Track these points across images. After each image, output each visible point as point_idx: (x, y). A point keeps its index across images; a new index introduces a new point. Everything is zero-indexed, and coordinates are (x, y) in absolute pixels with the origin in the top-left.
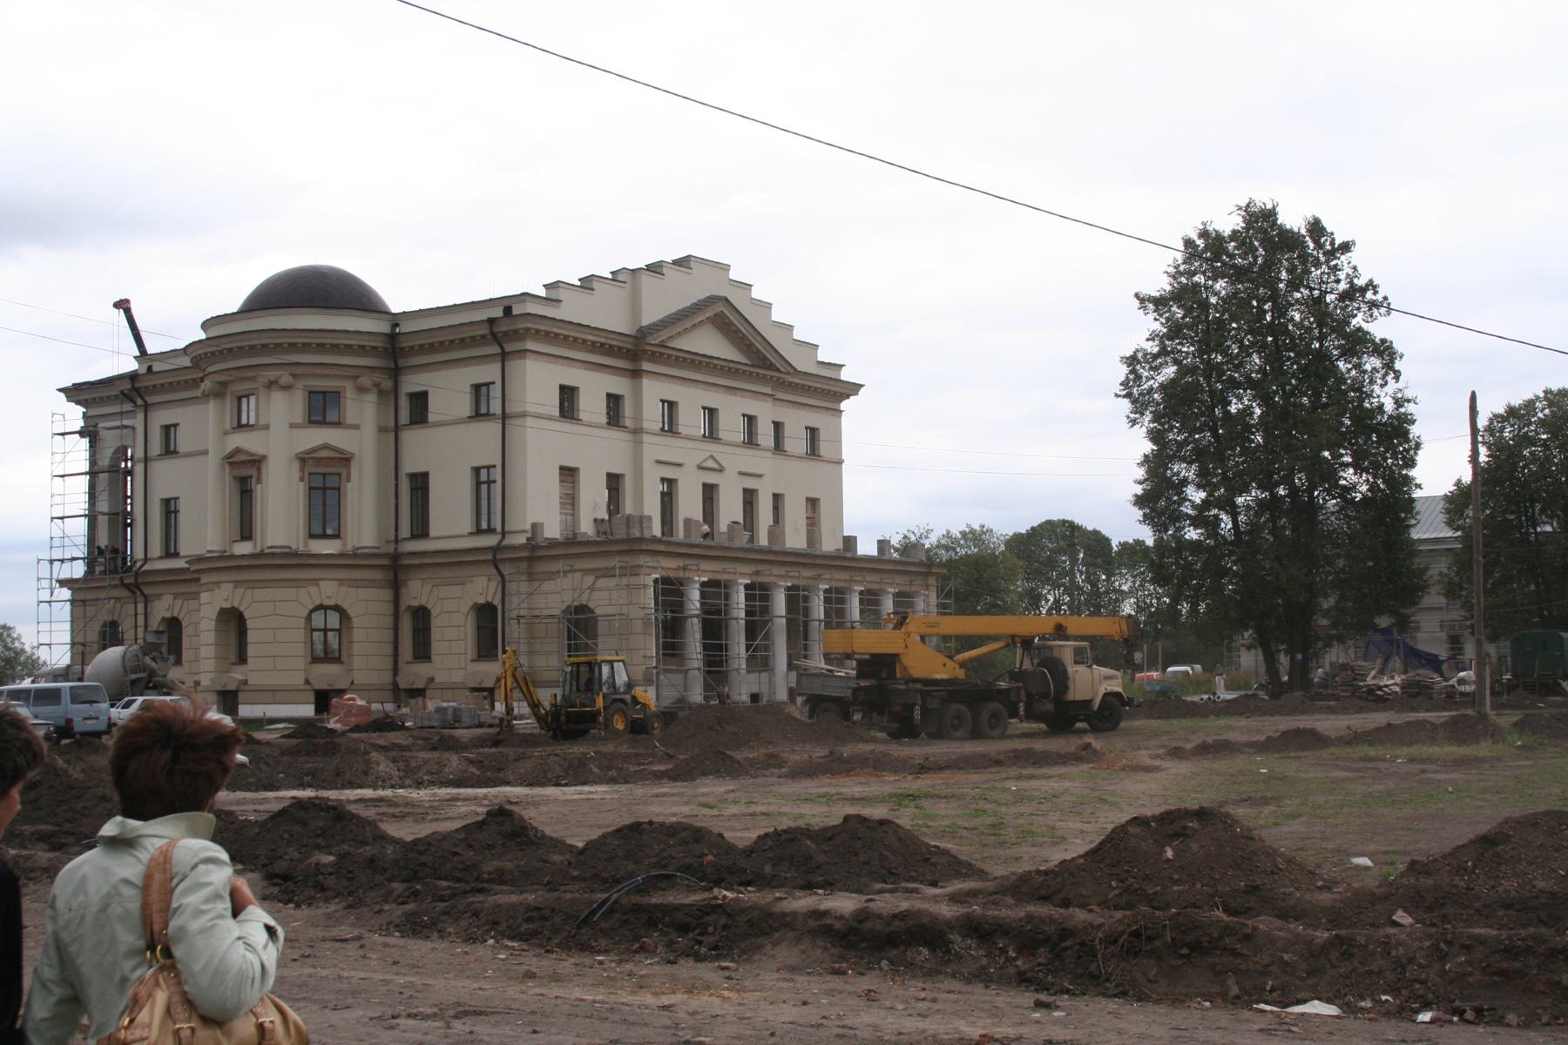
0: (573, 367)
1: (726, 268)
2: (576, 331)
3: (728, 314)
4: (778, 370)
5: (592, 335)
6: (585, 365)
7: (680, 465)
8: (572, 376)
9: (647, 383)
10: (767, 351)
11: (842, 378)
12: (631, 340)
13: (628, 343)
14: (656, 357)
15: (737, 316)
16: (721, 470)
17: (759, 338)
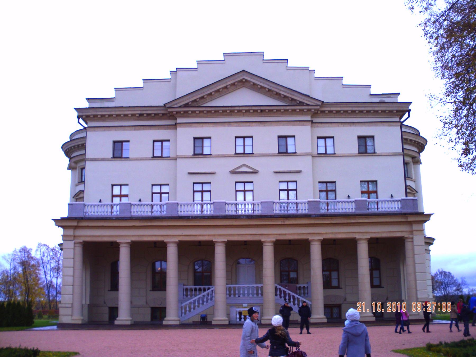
0: (105, 130)
1: (261, 54)
2: (116, 111)
3: (249, 79)
4: (308, 105)
5: (129, 111)
6: (133, 128)
7: (213, 173)
8: (120, 135)
9: (180, 130)
10: (292, 95)
11: (399, 101)
12: (163, 108)
13: (162, 110)
14: (186, 114)
15: (259, 79)
16: (255, 172)
17: (282, 89)
